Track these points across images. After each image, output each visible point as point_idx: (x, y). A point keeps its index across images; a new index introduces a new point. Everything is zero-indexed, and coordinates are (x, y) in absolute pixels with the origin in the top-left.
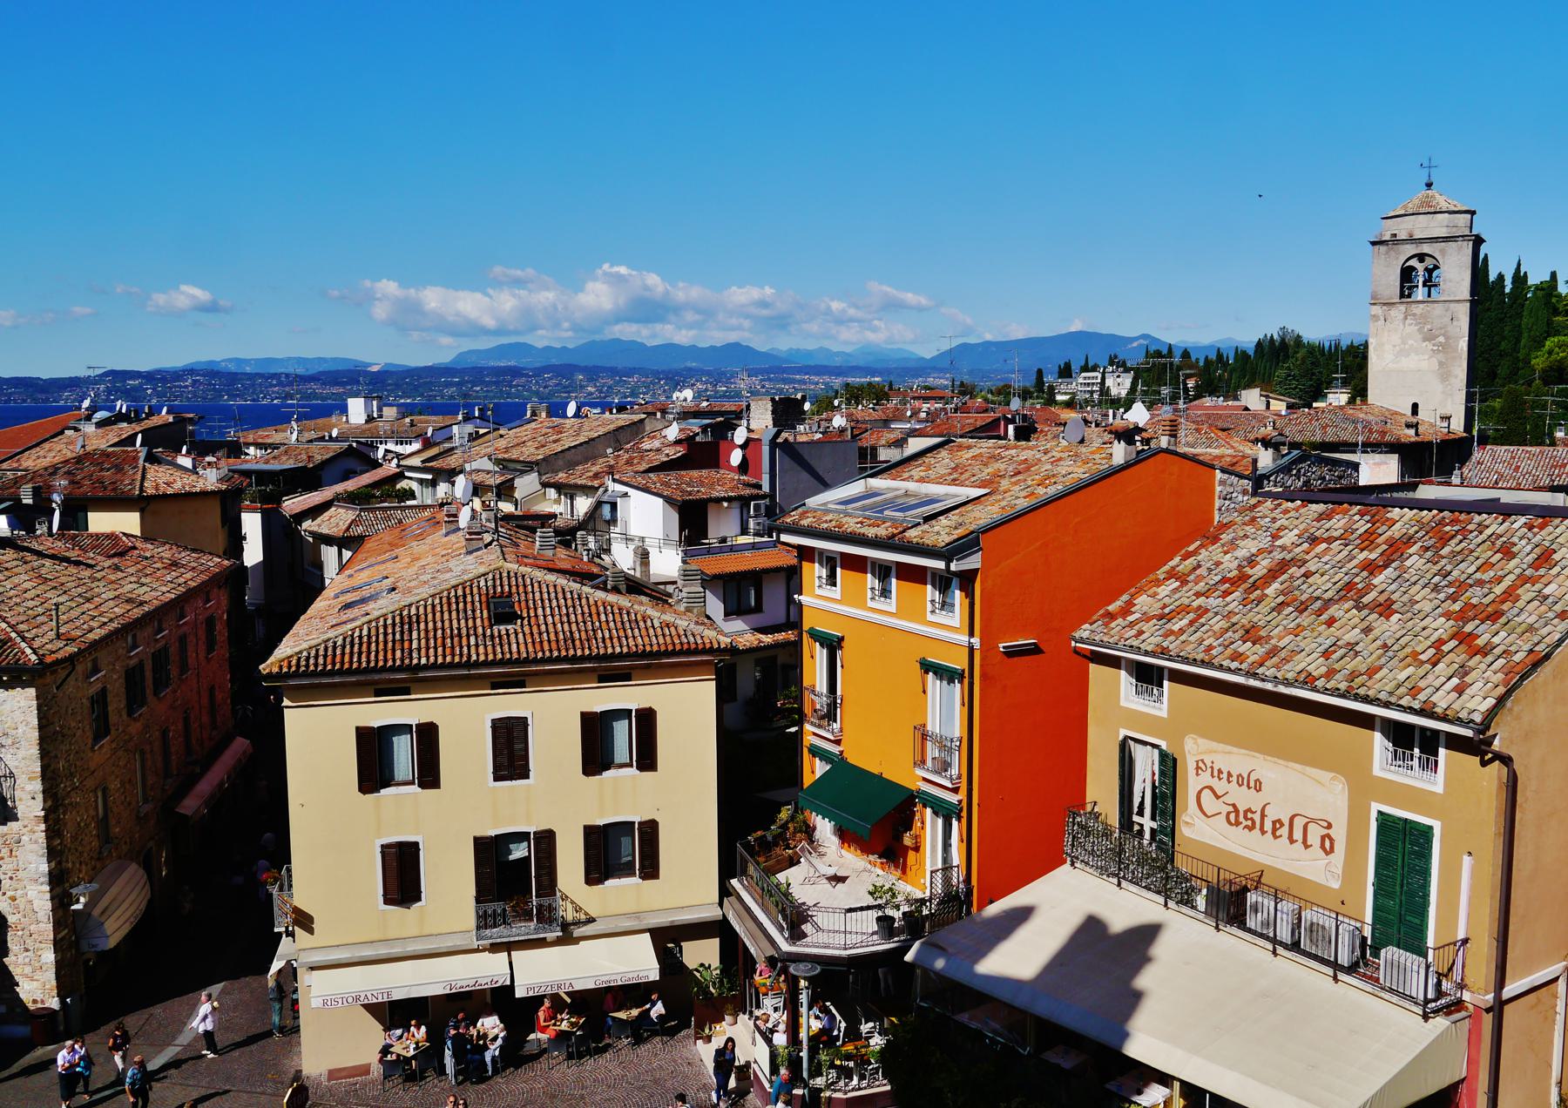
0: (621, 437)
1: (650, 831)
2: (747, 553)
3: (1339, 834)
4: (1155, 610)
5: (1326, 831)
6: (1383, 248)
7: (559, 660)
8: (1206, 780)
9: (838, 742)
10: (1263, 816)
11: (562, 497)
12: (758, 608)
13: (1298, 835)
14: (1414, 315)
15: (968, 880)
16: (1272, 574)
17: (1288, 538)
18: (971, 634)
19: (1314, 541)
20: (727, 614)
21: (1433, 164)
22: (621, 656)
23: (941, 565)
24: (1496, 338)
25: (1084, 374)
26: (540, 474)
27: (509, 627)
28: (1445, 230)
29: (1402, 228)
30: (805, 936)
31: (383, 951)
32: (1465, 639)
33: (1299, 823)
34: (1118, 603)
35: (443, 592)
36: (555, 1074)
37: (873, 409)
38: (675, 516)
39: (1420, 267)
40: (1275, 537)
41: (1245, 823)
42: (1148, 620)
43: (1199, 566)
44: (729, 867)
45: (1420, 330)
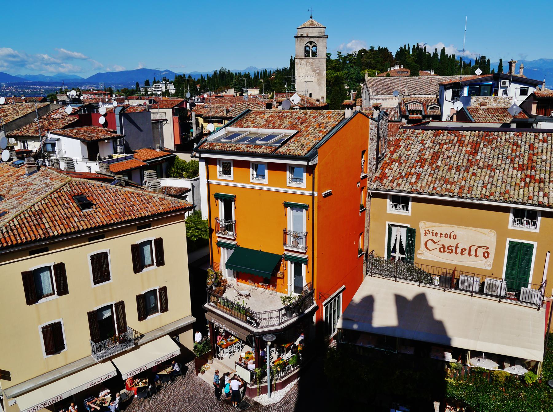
2: (124, 162)
5: (486, 250)
6: (299, 39)
7: (122, 223)
8: (430, 236)
9: (234, 240)
10: (457, 247)
11: (19, 142)
13: (473, 252)
14: (309, 63)
15: (312, 287)
18: (313, 191)
21: (312, 10)
22: (148, 217)
23: (305, 163)
25: (155, 84)
26: (5, 132)
28: (318, 33)
29: (304, 32)
31: (51, 378)
33: (473, 249)
35: (48, 196)
39: (311, 46)
41: (448, 251)
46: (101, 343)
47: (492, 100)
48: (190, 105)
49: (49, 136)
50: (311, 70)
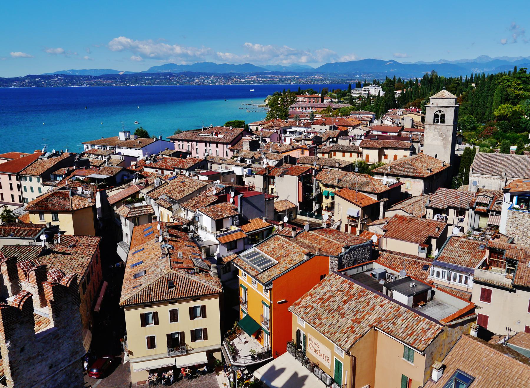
0: (201, 190)
1: (205, 330)
2: (233, 234)
3: (330, 359)
4: (304, 305)
12: (236, 247)
13: (324, 358)
15: (271, 348)
16: (327, 300)
18: (271, 300)
19: (338, 290)
20: (228, 250)
24: (486, 102)
25: (364, 87)
26: (179, 204)
27: (173, 289)
28: (447, 104)
30: (236, 360)
31: (148, 359)
32: (352, 327)
33: (324, 356)
34: (299, 300)
36: (186, 383)
38: (215, 222)
39: (440, 114)
40: (332, 287)
42: (303, 307)
43: (316, 293)
44: (222, 340)
45: (438, 133)
46: (171, 349)
47: (526, 215)
48: (315, 171)
49: (198, 212)
50: (438, 135)
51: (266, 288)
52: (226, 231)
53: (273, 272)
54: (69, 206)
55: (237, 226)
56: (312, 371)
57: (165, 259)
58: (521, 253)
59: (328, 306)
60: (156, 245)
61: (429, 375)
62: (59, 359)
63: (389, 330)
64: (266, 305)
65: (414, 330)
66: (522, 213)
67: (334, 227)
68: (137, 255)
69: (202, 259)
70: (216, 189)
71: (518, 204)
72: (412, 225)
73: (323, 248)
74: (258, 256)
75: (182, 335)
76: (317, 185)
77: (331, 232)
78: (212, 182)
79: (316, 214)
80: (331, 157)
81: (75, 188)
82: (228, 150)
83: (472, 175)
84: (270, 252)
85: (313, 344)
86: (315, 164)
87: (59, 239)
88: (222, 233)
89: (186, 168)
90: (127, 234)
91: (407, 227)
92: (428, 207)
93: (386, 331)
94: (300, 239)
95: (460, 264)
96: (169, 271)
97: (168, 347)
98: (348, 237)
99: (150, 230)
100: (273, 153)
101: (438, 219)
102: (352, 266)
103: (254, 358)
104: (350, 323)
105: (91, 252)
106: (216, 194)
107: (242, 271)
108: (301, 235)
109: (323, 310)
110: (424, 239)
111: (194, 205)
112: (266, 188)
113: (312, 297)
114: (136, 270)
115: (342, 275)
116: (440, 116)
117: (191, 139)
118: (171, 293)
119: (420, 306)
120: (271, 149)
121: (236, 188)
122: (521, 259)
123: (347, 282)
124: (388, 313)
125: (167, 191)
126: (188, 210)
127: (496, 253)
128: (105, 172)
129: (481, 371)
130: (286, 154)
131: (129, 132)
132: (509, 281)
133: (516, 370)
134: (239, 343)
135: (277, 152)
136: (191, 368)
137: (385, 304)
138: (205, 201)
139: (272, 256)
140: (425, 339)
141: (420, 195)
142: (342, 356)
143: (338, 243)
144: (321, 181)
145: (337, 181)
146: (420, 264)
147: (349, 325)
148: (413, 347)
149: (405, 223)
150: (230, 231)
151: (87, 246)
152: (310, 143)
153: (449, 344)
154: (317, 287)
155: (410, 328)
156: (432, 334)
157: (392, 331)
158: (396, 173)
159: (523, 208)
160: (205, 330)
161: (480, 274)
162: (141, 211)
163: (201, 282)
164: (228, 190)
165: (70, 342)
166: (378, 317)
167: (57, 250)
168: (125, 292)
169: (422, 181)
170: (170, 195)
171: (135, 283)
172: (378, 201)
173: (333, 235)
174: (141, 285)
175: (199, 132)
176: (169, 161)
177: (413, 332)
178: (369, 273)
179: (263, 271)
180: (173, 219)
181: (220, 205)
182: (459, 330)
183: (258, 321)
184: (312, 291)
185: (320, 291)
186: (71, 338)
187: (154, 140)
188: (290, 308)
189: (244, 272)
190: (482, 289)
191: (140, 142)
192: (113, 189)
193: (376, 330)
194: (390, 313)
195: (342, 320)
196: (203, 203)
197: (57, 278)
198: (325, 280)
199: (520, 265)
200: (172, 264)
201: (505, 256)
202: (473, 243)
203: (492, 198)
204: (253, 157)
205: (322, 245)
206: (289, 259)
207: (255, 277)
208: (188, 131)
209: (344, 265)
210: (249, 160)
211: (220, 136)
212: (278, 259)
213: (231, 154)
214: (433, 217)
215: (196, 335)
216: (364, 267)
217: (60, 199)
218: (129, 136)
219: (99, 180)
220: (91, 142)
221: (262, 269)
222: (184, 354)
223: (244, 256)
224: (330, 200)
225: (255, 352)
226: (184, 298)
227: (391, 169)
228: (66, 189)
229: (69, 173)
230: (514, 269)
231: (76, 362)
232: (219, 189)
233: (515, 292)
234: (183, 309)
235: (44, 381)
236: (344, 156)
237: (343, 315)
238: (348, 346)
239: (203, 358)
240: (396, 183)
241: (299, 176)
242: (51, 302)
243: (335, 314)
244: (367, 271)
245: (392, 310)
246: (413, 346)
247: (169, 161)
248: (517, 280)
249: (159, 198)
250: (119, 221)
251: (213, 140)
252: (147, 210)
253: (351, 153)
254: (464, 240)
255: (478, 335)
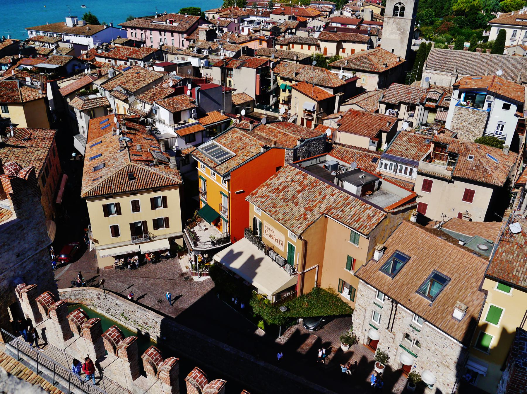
0: (157, 82)
1: (167, 219)
2: (191, 127)
3: (284, 243)
12: (194, 140)
15: (230, 234)
16: (282, 190)
17: (289, 179)
18: (229, 191)
19: (293, 181)
26: (135, 96)
31: (113, 246)
32: (305, 215)
33: (279, 240)
34: (255, 191)
36: (150, 267)
37: (244, 10)
38: (172, 115)
39: (399, 6)
40: (287, 178)
43: (272, 183)
44: (184, 227)
46: (134, 237)
47: (471, 111)
48: (273, 64)
49: (155, 104)
51: (224, 179)
52: (184, 124)
53: (231, 164)
54: (18, 97)
55: (195, 119)
56: (267, 253)
57: (124, 151)
58: (462, 147)
59: (283, 195)
60: (114, 138)
61: (371, 256)
62: (25, 248)
63: (338, 217)
64: (224, 195)
65: (361, 217)
66: (468, 109)
67: (290, 121)
68: (95, 148)
69: (161, 152)
70: (173, 81)
71: (465, 100)
72: (365, 119)
73: (279, 141)
74: (216, 148)
75: (145, 224)
76: (274, 79)
77: (287, 125)
78: (169, 74)
79: (273, 107)
80: (289, 49)
81: (22, 78)
82: (184, 40)
83: (426, 71)
84: (228, 144)
85: (269, 230)
86: (273, 56)
87: (12, 132)
88: (180, 126)
89: (141, 58)
90: (83, 127)
91: (360, 121)
92: (381, 102)
93: (335, 218)
94: (257, 132)
95: (407, 157)
96: (128, 164)
97: (132, 235)
98: (304, 131)
99: (106, 123)
100: (230, 44)
101: (390, 114)
102: (306, 159)
103: (213, 243)
104: (303, 210)
105: (47, 145)
106: (173, 86)
107: (201, 163)
108: (258, 128)
109: (278, 199)
110: (375, 133)
111: (151, 97)
112: (223, 80)
113: (268, 188)
114: (95, 163)
115: (296, 167)
116: (399, 9)
117: (144, 26)
118: (131, 184)
119: (367, 195)
120: (228, 40)
121: (193, 80)
122: (462, 153)
123: (301, 173)
124: (338, 202)
125: (121, 83)
126: (144, 103)
127: (440, 146)
128: (53, 61)
129: (416, 252)
130: (244, 45)
131: (76, 17)
132: (449, 173)
133: (447, 250)
134: (199, 230)
135: (235, 43)
136: (155, 253)
137: (336, 193)
138: (161, 93)
139: (230, 148)
140: (370, 225)
141: (374, 90)
142: (295, 239)
143: (294, 136)
144: (278, 74)
145: (294, 75)
146: (370, 157)
147: (302, 213)
148: (359, 232)
149: (359, 117)
150: (188, 124)
151: (42, 139)
152: (268, 34)
153: (391, 228)
154: (273, 178)
155: (357, 215)
156: (377, 220)
157: (341, 218)
158: (353, 68)
159: (469, 105)
160: (167, 219)
161: (423, 166)
162: (96, 104)
163: (161, 174)
164: (185, 82)
165: (35, 232)
166: (329, 205)
167: (11, 144)
168: (86, 185)
169: (377, 77)
170: (125, 87)
171: (95, 175)
172: (334, 95)
173: (289, 129)
174: (101, 177)
175: (152, 20)
176: (122, 50)
177: (360, 219)
178: (322, 165)
179: (222, 163)
180: (130, 112)
181: (177, 97)
182: (400, 216)
183: (217, 210)
184: (268, 181)
185: (276, 181)
186: (35, 228)
187: (105, 27)
188: (248, 198)
189: (203, 164)
190: (425, 180)
191: (89, 29)
192: (64, 80)
193: (326, 217)
194: (340, 202)
195: (296, 209)
196: (160, 95)
197: (14, 172)
198: (281, 171)
199: (460, 158)
200: (131, 156)
201: (447, 150)
202: (420, 138)
203: (442, 94)
204: (210, 48)
205: (278, 138)
206: (246, 151)
207: (213, 169)
208: (141, 18)
209: (299, 157)
210: (206, 51)
211: (175, 24)
212: (235, 151)
213: (187, 43)
214: (385, 112)
215: (158, 224)
216: (318, 159)
217: (7, 90)
218: (77, 22)
219: (49, 70)
220: (35, 28)
221: (220, 161)
222: (147, 241)
223: (202, 149)
224: (287, 94)
225: (215, 238)
226: (145, 189)
227: (347, 63)
228: (13, 80)
229: (14, 62)
230: (454, 161)
231: (43, 250)
232: (176, 81)
233: (453, 182)
234: (144, 199)
235: (12, 268)
236: (302, 48)
237: (296, 204)
238: (300, 231)
239: (165, 245)
240: (352, 78)
241: (257, 69)
242: (10, 194)
243: (290, 203)
244: (320, 163)
245: (342, 199)
246: (359, 230)
247: (122, 50)
248: (456, 172)
249: (114, 89)
250: (72, 113)
251: (167, 28)
252: (102, 102)
253: (309, 45)
254: (412, 134)
255: (417, 221)
